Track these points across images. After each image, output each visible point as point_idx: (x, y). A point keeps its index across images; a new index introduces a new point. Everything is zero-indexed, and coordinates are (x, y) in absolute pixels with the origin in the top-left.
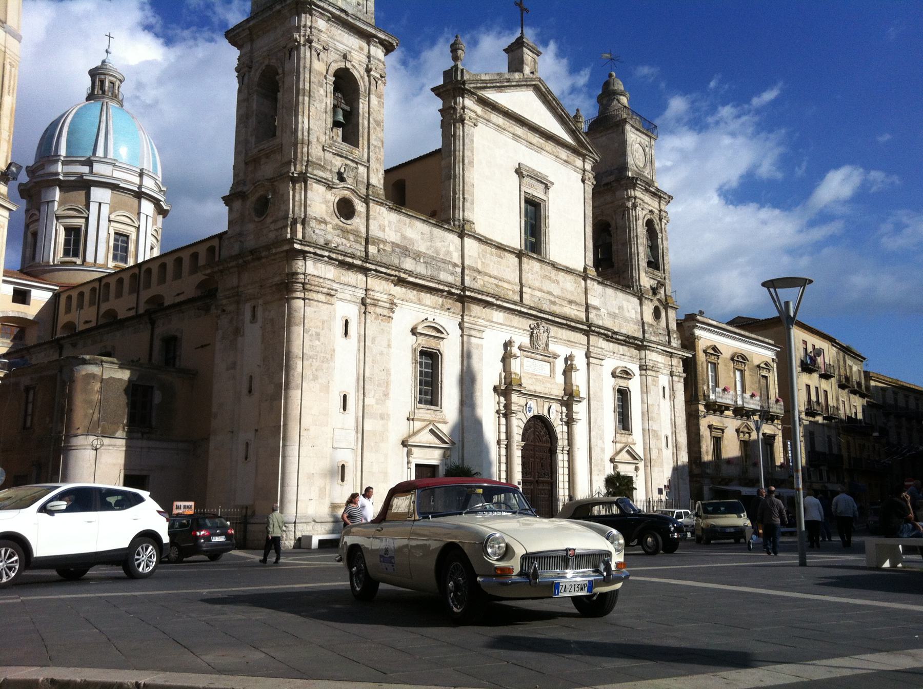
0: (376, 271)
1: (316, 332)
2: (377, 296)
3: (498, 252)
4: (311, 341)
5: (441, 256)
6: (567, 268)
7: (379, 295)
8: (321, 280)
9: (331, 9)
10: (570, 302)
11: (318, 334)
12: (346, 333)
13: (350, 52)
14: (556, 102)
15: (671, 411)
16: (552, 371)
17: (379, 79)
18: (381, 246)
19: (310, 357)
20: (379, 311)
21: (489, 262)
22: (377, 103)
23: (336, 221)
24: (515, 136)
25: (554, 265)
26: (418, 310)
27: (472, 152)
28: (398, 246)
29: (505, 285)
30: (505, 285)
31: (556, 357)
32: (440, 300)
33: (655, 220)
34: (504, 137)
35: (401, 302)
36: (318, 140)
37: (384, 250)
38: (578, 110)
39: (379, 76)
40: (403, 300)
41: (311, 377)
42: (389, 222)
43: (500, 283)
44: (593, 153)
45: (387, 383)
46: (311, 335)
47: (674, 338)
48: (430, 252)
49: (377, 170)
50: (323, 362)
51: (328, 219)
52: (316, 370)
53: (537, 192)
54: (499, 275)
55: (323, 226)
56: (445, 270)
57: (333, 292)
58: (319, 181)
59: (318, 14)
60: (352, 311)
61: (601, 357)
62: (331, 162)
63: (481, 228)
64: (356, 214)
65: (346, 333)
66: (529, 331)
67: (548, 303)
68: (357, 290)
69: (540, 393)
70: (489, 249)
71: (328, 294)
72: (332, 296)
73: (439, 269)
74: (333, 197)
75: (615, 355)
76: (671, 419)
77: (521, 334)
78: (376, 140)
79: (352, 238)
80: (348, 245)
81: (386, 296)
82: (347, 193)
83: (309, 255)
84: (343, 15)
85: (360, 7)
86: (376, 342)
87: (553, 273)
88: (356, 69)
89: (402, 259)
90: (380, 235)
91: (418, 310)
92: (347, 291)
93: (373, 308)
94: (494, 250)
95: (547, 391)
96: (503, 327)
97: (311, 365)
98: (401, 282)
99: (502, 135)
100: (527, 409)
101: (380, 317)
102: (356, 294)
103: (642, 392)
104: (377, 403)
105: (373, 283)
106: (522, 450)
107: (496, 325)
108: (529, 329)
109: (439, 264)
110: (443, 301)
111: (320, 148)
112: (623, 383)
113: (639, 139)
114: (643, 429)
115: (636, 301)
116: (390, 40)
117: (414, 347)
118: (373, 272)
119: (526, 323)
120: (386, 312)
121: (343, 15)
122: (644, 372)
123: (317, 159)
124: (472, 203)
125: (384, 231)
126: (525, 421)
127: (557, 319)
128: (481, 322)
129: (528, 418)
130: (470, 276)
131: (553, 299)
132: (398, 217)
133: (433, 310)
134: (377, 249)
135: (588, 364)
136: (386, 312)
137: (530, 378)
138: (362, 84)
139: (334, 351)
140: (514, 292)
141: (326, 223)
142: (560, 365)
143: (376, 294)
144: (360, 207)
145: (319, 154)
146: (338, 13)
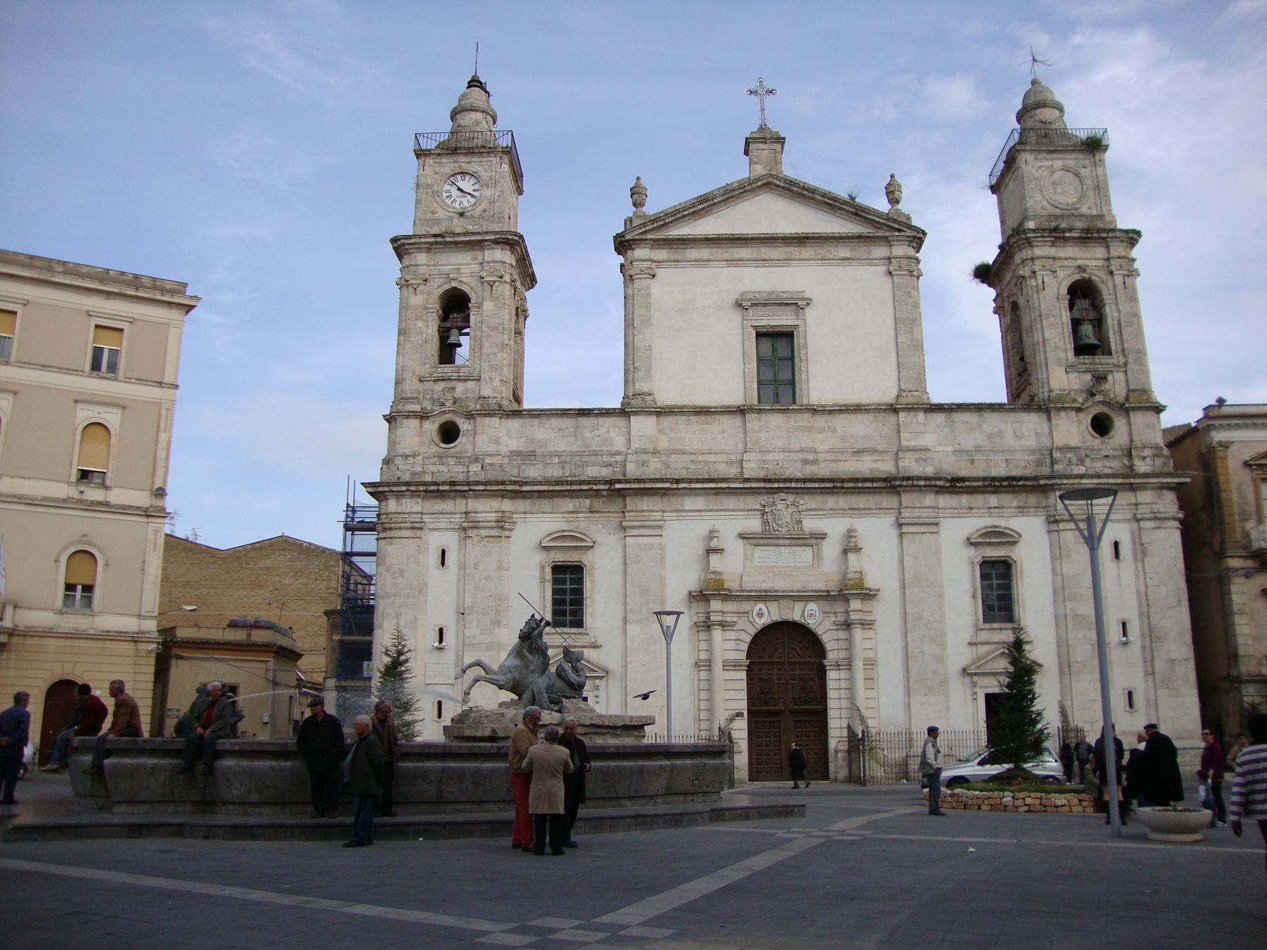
0: (471, 490)
1: (399, 569)
2: (481, 516)
3: (703, 418)
4: (393, 579)
5: (594, 448)
6: (846, 406)
7: (484, 515)
8: (406, 516)
9: (423, 240)
10: (859, 452)
11: (401, 572)
12: (443, 563)
13: (459, 269)
14: (807, 190)
15: (1137, 577)
16: (817, 557)
17: (495, 282)
18: (488, 460)
19: (393, 595)
20: (484, 532)
21: (683, 435)
22: (492, 308)
23: (434, 449)
24: (731, 262)
25: (815, 411)
26: (550, 519)
27: (648, 307)
28: (518, 453)
29: (712, 458)
30: (712, 458)
31: (822, 537)
32: (587, 502)
33: (1094, 278)
34: (711, 269)
35: (523, 516)
36: (413, 372)
37: (490, 464)
38: (892, 176)
39: (494, 278)
40: (525, 513)
41: (393, 615)
42: (509, 431)
43: (701, 458)
44: (900, 231)
45: (496, 609)
46: (393, 573)
47: (1144, 458)
48: (574, 449)
49: (491, 378)
50: (408, 597)
51: (422, 450)
52: (400, 607)
53: (780, 319)
54: (704, 447)
55: (411, 460)
56: (594, 464)
57: (417, 525)
58: (408, 417)
59: (415, 251)
60: (450, 540)
62: (433, 390)
63: (666, 397)
64: (461, 434)
65: (443, 563)
66: (758, 510)
67: (799, 465)
68: (454, 516)
69: (784, 591)
70: (681, 419)
71: (413, 528)
72: (421, 529)
73: (586, 464)
74: (432, 427)
75: (974, 511)
76: (1138, 592)
78: (490, 347)
79: (451, 461)
80: (446, 470)
81: (494, 515)
82: (448, 417)
83: (387, 494)
84: (439, 239)
85: (485, 214)
86: (480, 568)
87: (821, 421)
88: (465, 283)
89: (523, 467)
90: (492, 448)
91: (550, 519)
92: (442, 520)
93: (475, 531)
94: (693, 418)
95: (799, 586)
97: (394, 603)
98: (515, 495)
99: (707, 269)
100: (755, 614)
101: (486, 539)
102: (453, 520)
103: (1053, 558)
104: (481, 634)
105: (472, 504)
106: (747, 671)
107: (690, 514)
109: (585, 459)
110: (591, 502)
111: (416, 381)
112: (995, 553)
113: (1058, 164)
114: (1055, 616)
115: (1044, 417)
116: (502, 236)
117: (543, 563)
118: (471, 493)
119: (753, 502)
120: (494, 532)
121: (439, 239)
122: (1054, 527)
123: (412, 394)
124: (649, 370)
125: (497, 442)
126: (753, 632)
127: (808, 485)
128: (658, 515)
129: (759, 628)
130: (636, 462)
131: (810, 457)
132: (522, 420)
133: (575, 515)
134: (480, 469)
136: (494, 532)
138: (473, 294)
139: (426, 584)
140: (730, 463)
141: (414, 456)
142: (830, 549)
143: (479, 515)
144: (464, 425)
145: (414, 388)
146: (433, 240)
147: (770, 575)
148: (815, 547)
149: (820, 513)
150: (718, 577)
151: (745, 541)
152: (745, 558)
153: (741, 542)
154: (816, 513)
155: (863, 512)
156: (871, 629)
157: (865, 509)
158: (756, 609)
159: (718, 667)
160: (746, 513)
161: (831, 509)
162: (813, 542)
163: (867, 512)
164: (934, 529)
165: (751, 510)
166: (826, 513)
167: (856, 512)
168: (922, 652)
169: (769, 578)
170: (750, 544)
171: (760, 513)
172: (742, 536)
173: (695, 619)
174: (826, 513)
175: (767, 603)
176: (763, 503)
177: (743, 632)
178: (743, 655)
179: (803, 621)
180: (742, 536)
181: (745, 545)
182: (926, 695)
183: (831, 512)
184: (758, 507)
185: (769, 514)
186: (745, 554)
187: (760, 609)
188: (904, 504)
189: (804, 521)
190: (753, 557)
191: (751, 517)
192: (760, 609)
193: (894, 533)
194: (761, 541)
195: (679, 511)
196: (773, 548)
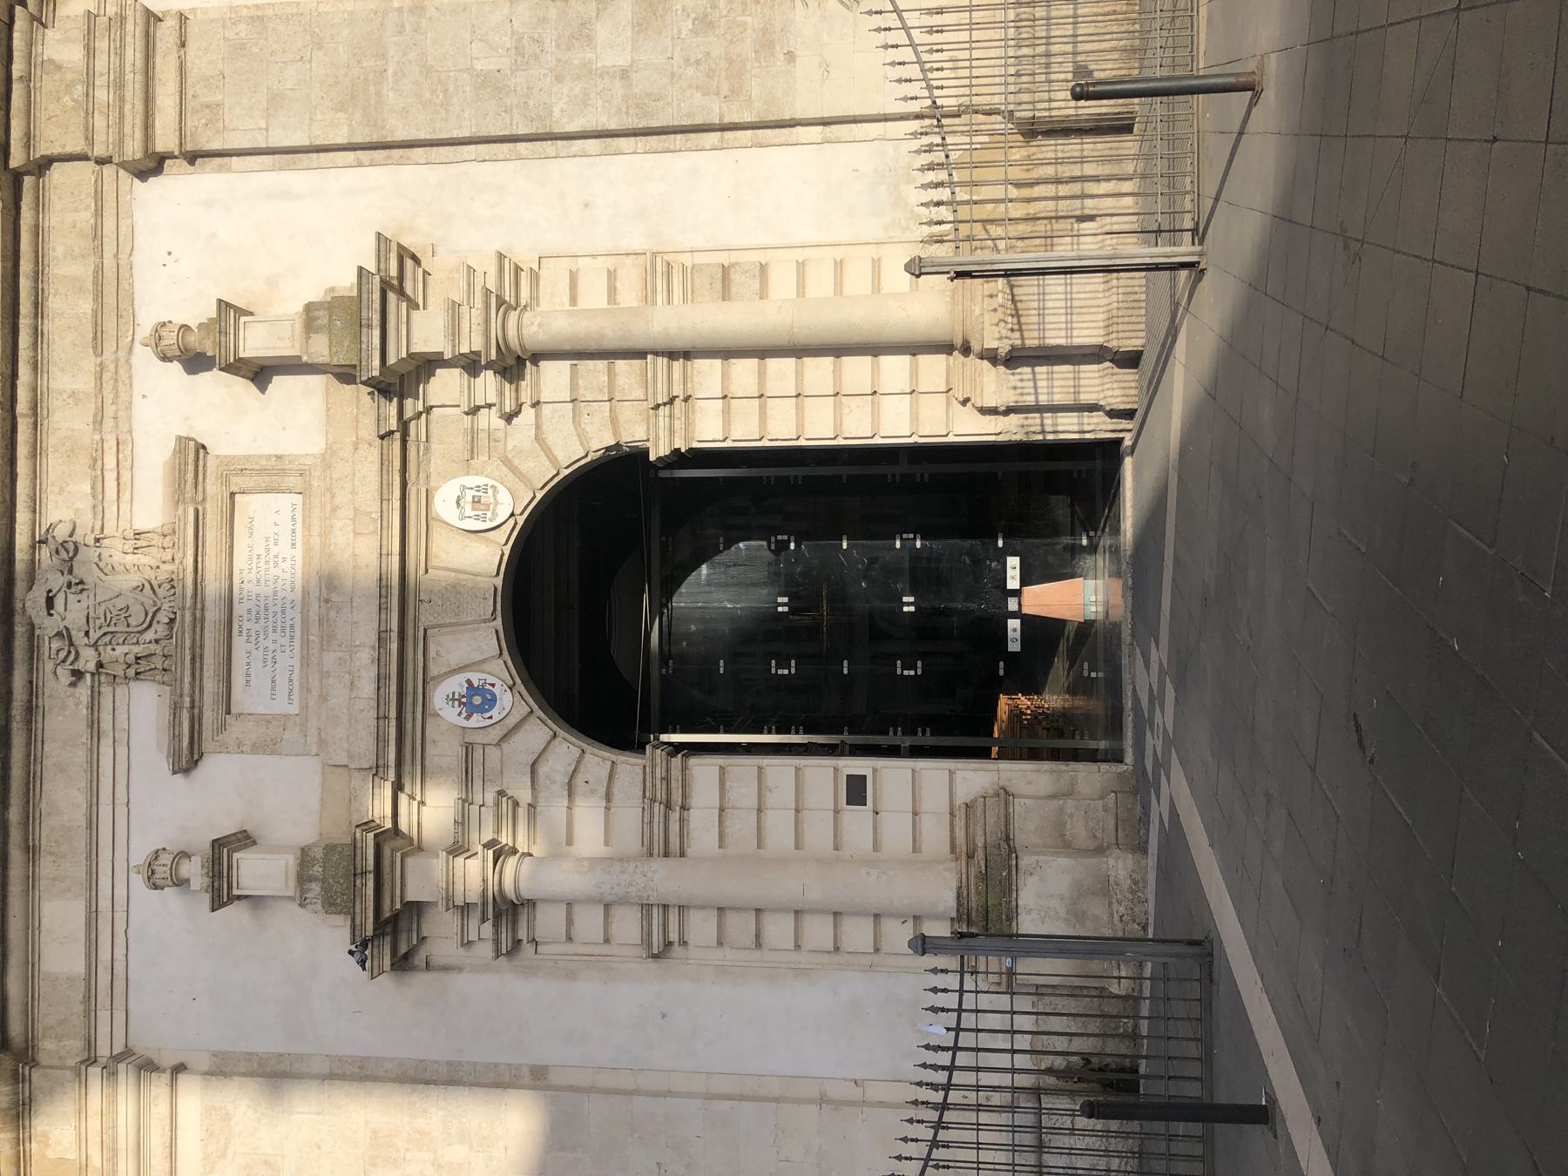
61: (134, 29)
66: (95, 695)
77: (122, 751)
96: (104, 904)
107: (104, 955)
108: (83, 691)
135: (193, 157)
137: (324, 698)
147: (330, 658)
148: (238, 482)
149: (110, 462)
150: (317, 870)
151: (207, 745)
152: (268, 747)
153: (215, 766)
154: (110, 477)
155: (110, 299)
156: (535, 277)
157: (99, 294)
158: (450, 714)
159: (665, 879)
160: (106, 744)
161: (98, 423)
162: (213, 488)
163: (110, 290)
164: (166, 35)
165: (94, 725)
166: (110, 445)
167: (110, 325)
168: (624, 74)
169: (341, 661)
170: (223, 727)
171: (106, 690)
172: (187, 759)
173: (485, 950)
174: (110, 445)
175: (434, 671)
176: (65, 677)
177: (543, 770)
178: (630, 767)
179: (501, 535)
180: (187, 759)
181: (224, 748)
182: (790, 56)
183: (108, 423)
184: (83, 691)
185: (108, 654)
186: (255, 749)
187: (452, 699)
188: (75, 145)
189: (140, 525)
190: (268, 720)
191: (122, 723)
192: (452, 699)
193: (175, 185)
194: (210, 685)
195: (90, 997)
196: (239, 643)
